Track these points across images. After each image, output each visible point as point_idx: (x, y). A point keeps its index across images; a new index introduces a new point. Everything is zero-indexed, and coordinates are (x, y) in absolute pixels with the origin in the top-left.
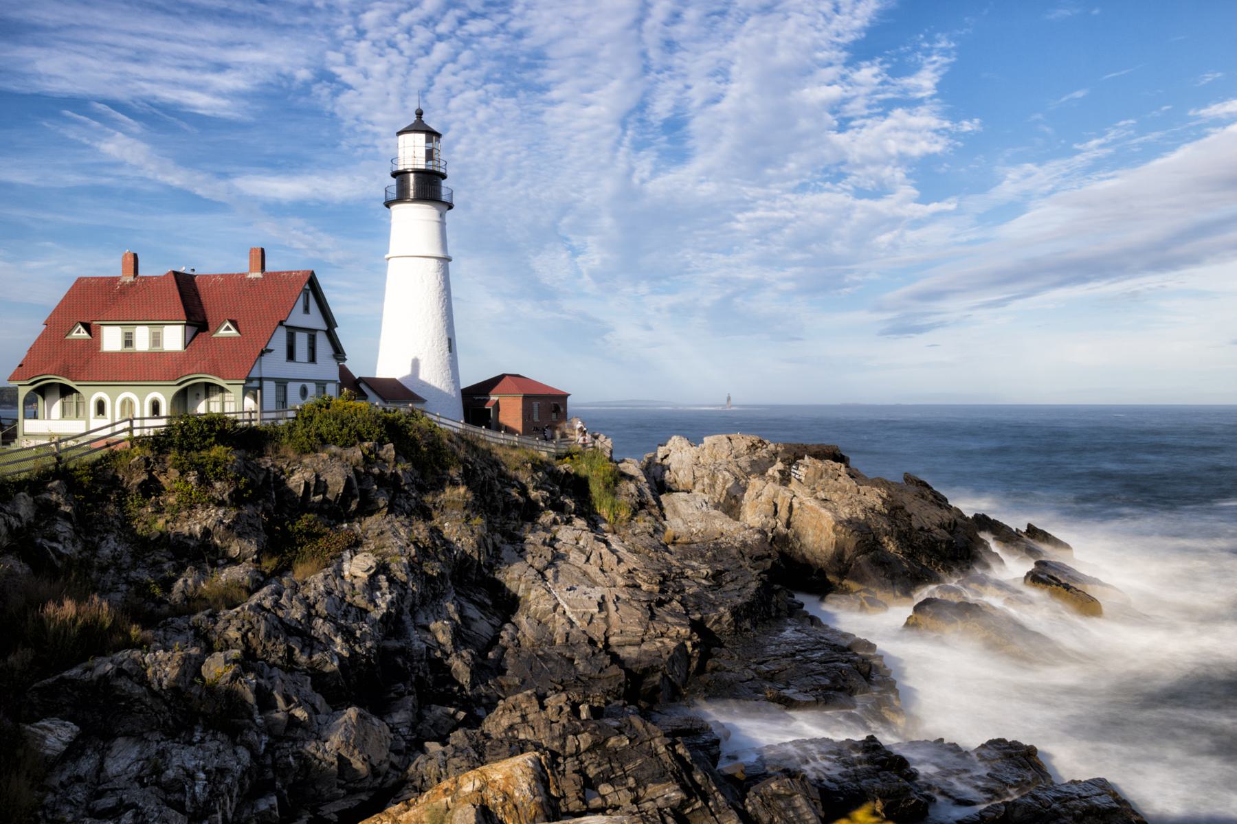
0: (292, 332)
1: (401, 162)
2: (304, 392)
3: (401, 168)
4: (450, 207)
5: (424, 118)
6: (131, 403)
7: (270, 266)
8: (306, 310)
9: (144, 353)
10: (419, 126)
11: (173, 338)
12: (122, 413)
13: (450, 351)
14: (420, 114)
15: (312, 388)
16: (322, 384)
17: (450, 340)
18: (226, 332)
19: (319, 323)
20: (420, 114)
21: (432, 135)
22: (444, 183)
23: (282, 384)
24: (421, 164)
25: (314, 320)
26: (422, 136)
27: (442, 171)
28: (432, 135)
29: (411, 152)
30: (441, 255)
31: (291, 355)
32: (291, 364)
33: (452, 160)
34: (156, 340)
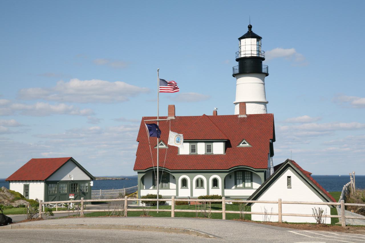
1: (242, 53)
3: (242, 56)
5: (253, 30)
6: (202, 181)
9: (203, 155)
10: (250, 34)
11: (218, 148)
12: (197, 185)
14: (250, 27)
20: (250, 27)
21: (259, 38)
22: (263, 62)
24: (255, 54)
26: (255, 39)
27: (263, 57)
28: (259, 38)
29: (249, 48)
30: (262, 100)
34: (209, 149)
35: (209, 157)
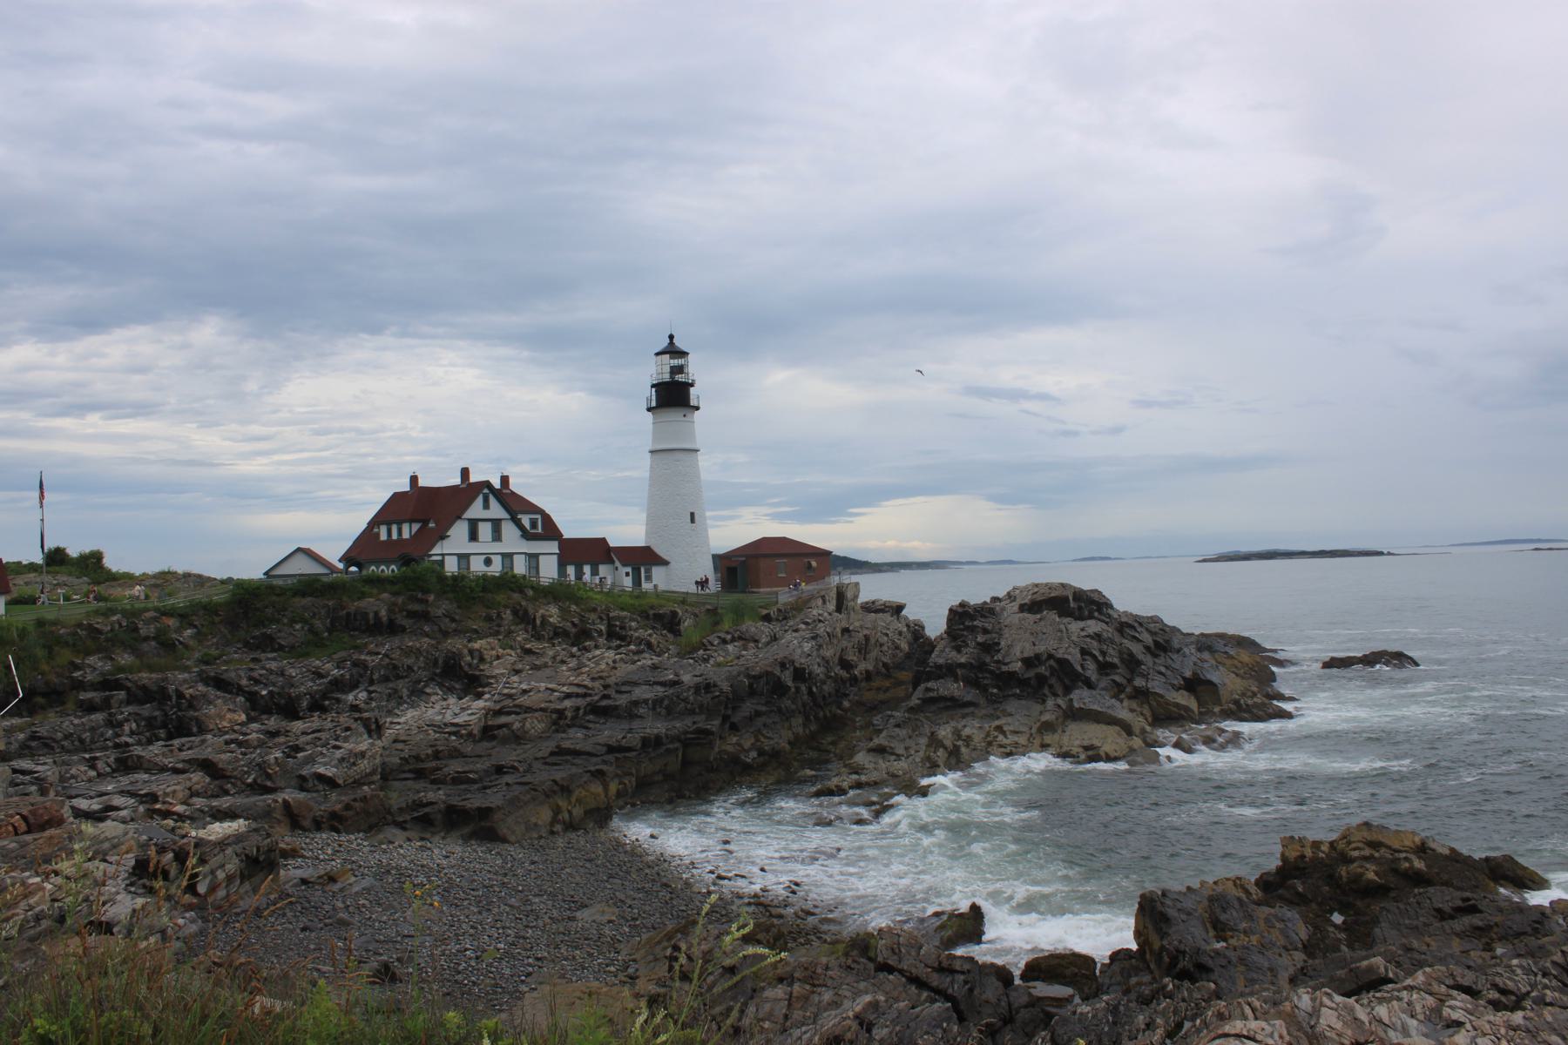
0: (473, 525)
2: (488, 562)
4: (697, 408)
7: (473, 478)
8: (486, 506)
13: (693, 521)
14: (671, 337)
15: (497, 560)
16: (508, 557)
17: (692, 515)
18: (432, 525)
19: (507, 516)
20: (671, 337)
22: (692, 390)
23: (464, 558)
25: (496, 511)
31: (473, 536)
32: (473, 544)
33: (698, 371)
34: (400, 532)
35: (400, 540)
